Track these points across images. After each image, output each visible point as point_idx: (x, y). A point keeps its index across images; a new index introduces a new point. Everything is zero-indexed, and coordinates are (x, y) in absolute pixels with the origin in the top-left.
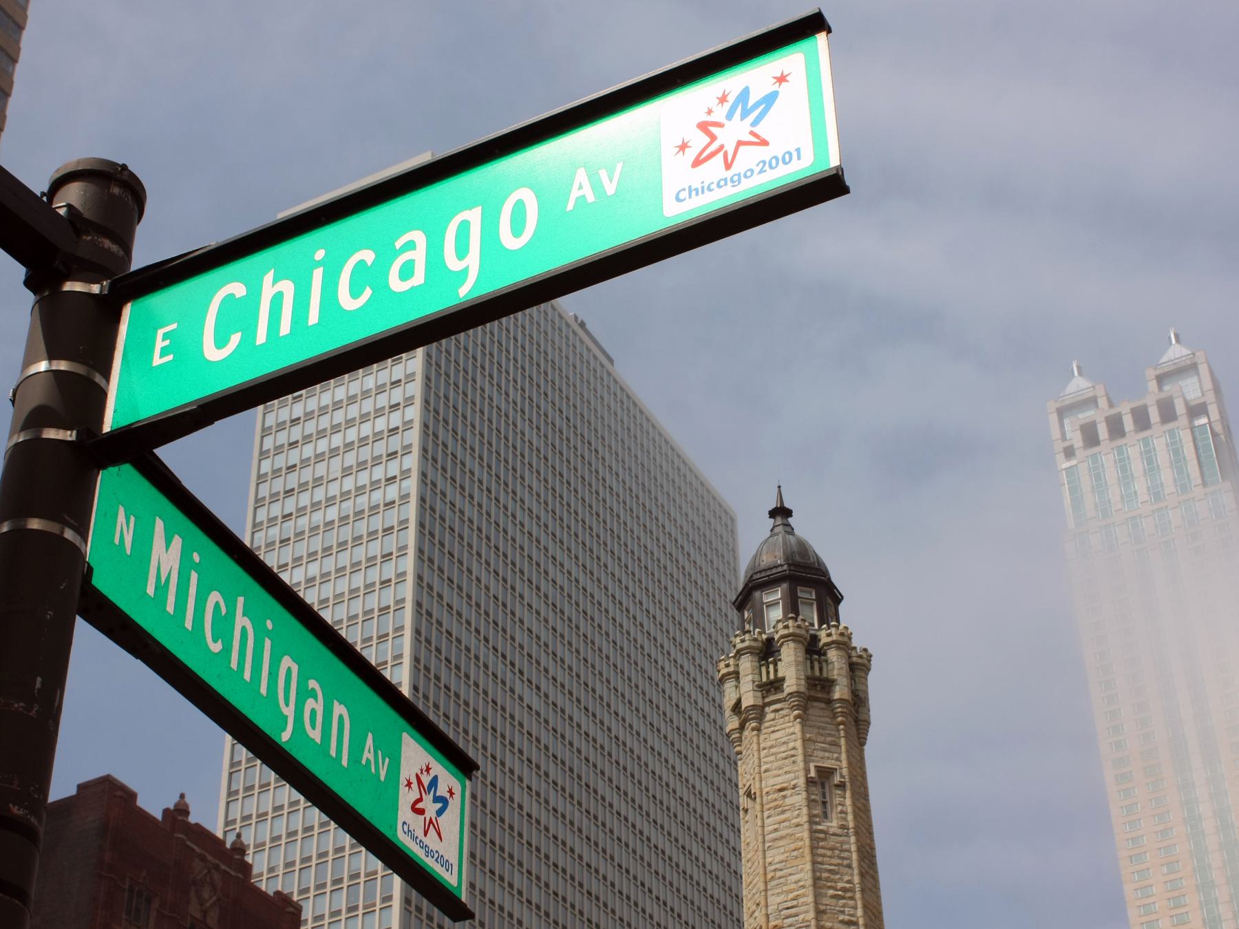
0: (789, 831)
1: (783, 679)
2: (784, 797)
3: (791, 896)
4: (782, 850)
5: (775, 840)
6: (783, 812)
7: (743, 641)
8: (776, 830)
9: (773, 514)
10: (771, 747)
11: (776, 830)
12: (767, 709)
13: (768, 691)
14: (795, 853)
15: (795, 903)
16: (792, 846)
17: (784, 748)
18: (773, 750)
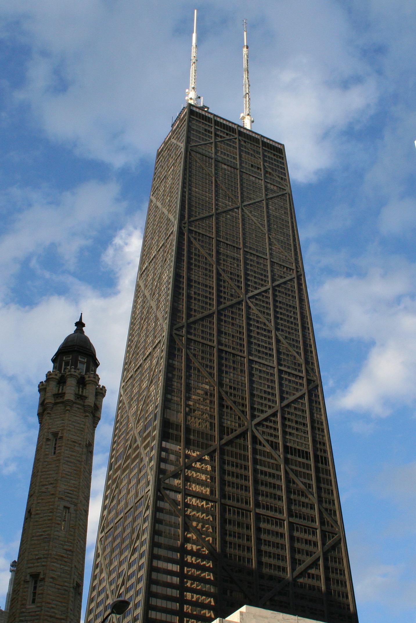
0: (75, 461)
1: (86, 398)
2: (75, 446)
3: (70, 488)
4: (70, 467)
5: (67, 461)
6: (73, 452)
7: (75, 372)
8: (69, 457)
9: (77, 324)
10: (73, 422)
11: (69, 457)
12: (74, 405)
13: (78, 398)
14: (75, 472)
15: (72, 492)
16: (75, 468)
17: (79, 425)
18: (74, 424)
